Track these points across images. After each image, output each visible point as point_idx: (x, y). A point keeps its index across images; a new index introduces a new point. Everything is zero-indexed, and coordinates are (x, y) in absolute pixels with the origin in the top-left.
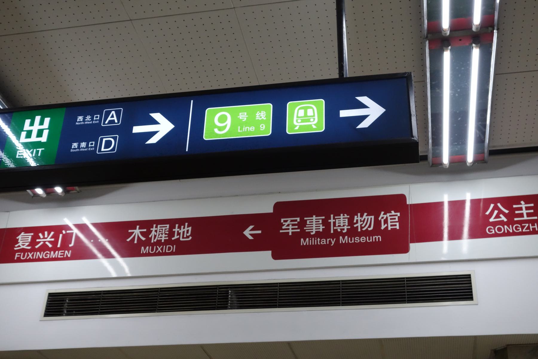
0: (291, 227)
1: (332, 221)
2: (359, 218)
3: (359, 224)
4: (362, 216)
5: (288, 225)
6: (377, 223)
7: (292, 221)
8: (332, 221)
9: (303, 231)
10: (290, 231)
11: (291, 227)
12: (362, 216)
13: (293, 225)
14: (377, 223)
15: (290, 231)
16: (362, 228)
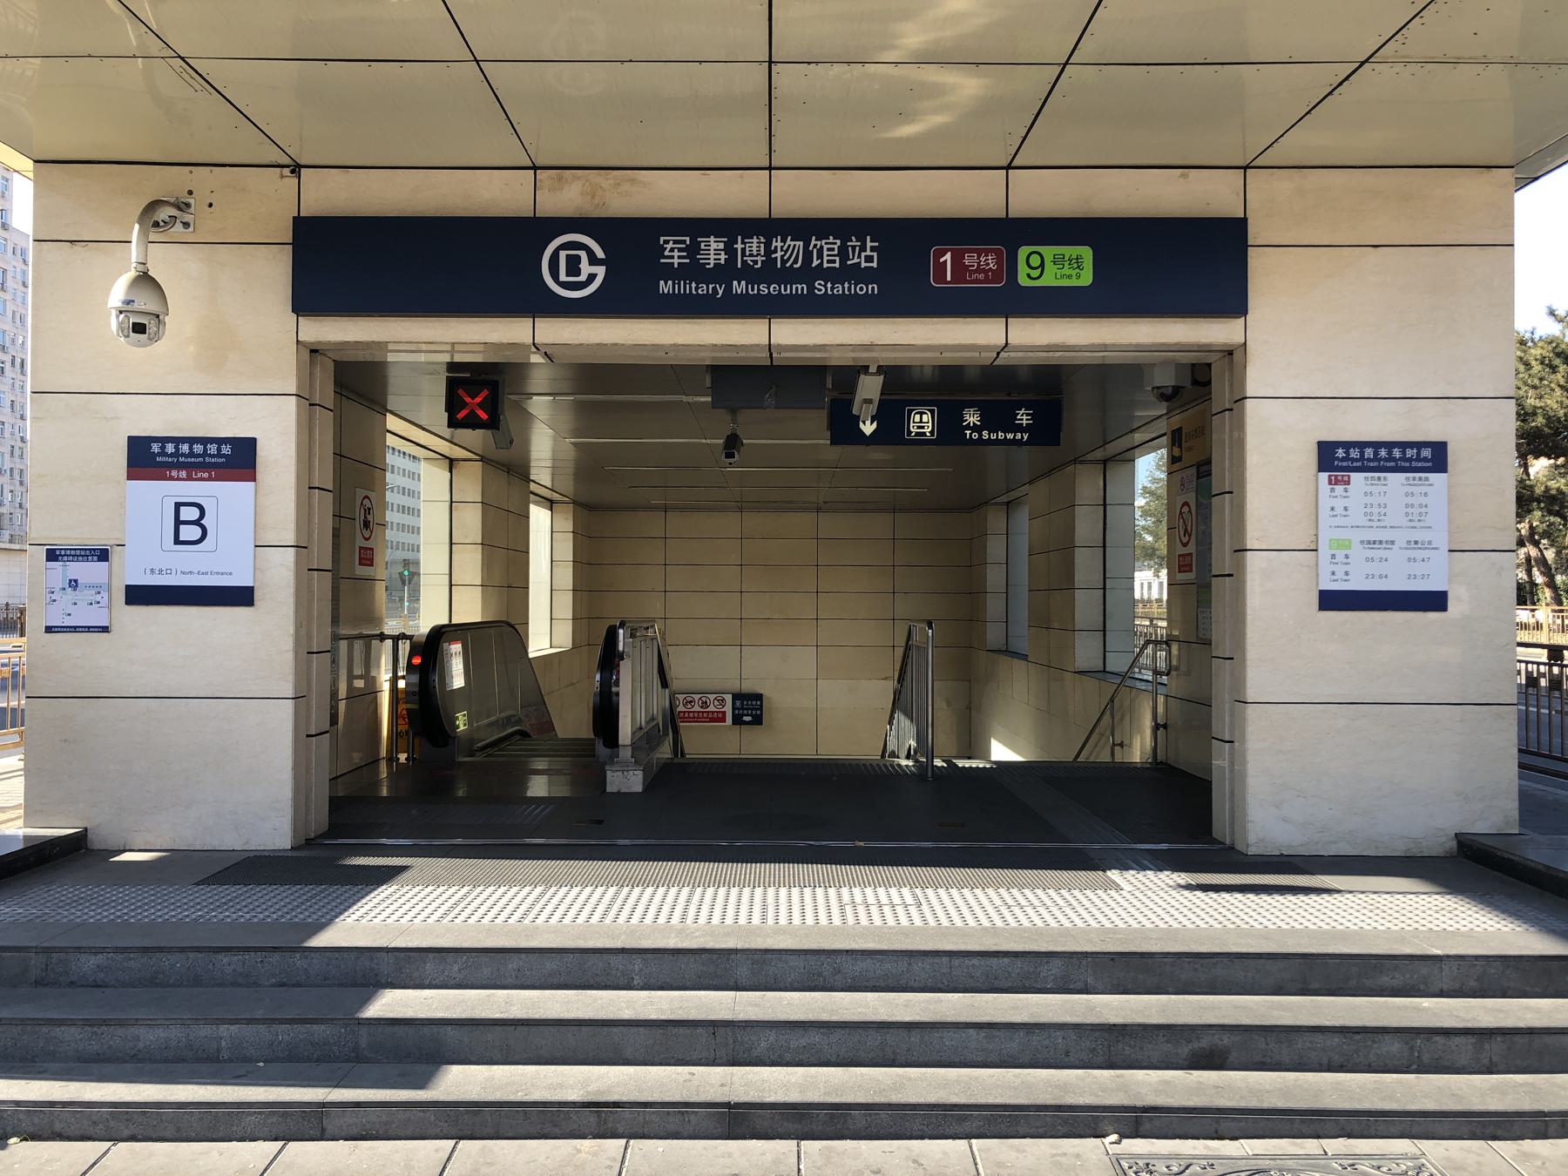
0: (676, 254)
1: (739, 246)
2: (779, 244)
3: (779, 254)
4: (784, 241)
5: (672, 250)
6: (808, 256)
7: (675, 242)
8: (739, 246)
9: (694, 261)
10: (676, 261)
11: (676, 254)
12: (784, 241)
13: (680, 250)
14: (808, 256)
15: (676, 261)
16: (784, 262)
